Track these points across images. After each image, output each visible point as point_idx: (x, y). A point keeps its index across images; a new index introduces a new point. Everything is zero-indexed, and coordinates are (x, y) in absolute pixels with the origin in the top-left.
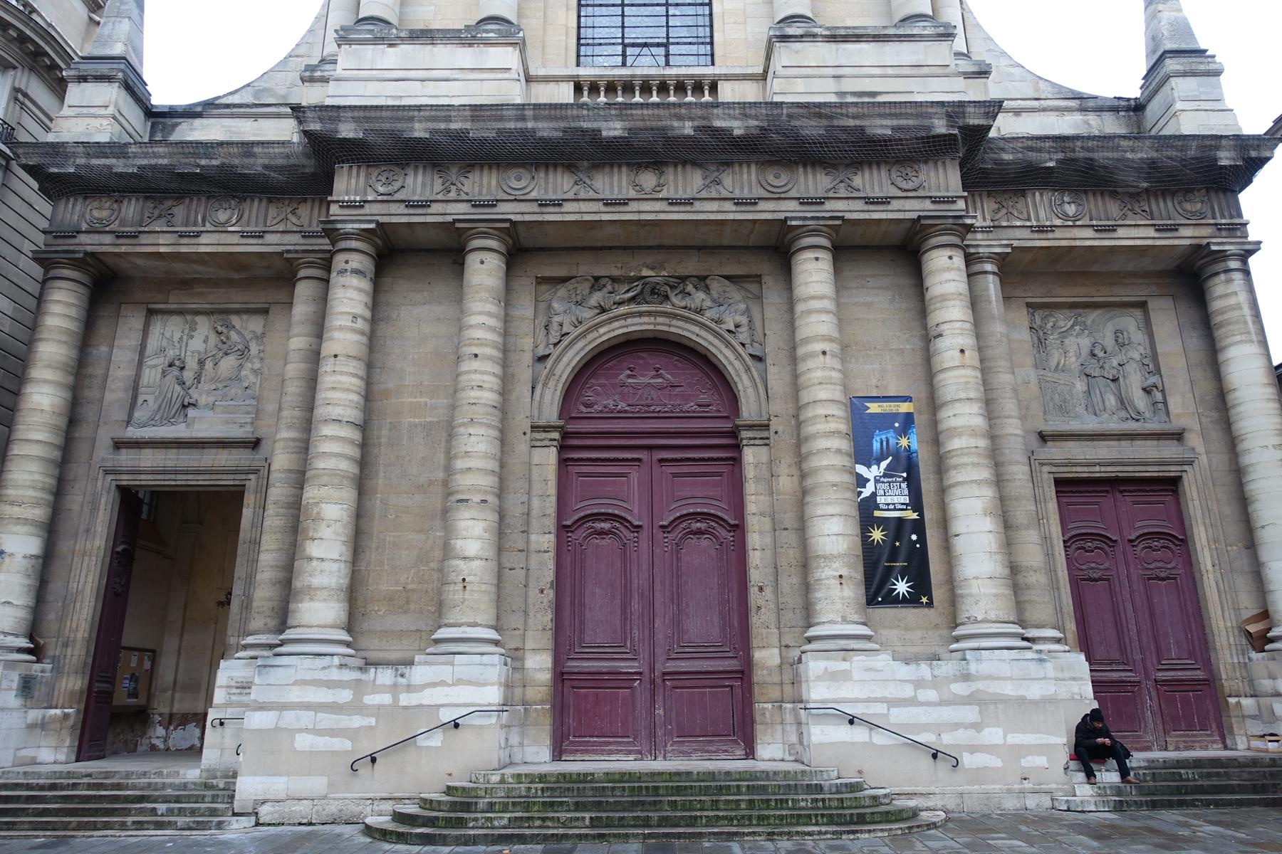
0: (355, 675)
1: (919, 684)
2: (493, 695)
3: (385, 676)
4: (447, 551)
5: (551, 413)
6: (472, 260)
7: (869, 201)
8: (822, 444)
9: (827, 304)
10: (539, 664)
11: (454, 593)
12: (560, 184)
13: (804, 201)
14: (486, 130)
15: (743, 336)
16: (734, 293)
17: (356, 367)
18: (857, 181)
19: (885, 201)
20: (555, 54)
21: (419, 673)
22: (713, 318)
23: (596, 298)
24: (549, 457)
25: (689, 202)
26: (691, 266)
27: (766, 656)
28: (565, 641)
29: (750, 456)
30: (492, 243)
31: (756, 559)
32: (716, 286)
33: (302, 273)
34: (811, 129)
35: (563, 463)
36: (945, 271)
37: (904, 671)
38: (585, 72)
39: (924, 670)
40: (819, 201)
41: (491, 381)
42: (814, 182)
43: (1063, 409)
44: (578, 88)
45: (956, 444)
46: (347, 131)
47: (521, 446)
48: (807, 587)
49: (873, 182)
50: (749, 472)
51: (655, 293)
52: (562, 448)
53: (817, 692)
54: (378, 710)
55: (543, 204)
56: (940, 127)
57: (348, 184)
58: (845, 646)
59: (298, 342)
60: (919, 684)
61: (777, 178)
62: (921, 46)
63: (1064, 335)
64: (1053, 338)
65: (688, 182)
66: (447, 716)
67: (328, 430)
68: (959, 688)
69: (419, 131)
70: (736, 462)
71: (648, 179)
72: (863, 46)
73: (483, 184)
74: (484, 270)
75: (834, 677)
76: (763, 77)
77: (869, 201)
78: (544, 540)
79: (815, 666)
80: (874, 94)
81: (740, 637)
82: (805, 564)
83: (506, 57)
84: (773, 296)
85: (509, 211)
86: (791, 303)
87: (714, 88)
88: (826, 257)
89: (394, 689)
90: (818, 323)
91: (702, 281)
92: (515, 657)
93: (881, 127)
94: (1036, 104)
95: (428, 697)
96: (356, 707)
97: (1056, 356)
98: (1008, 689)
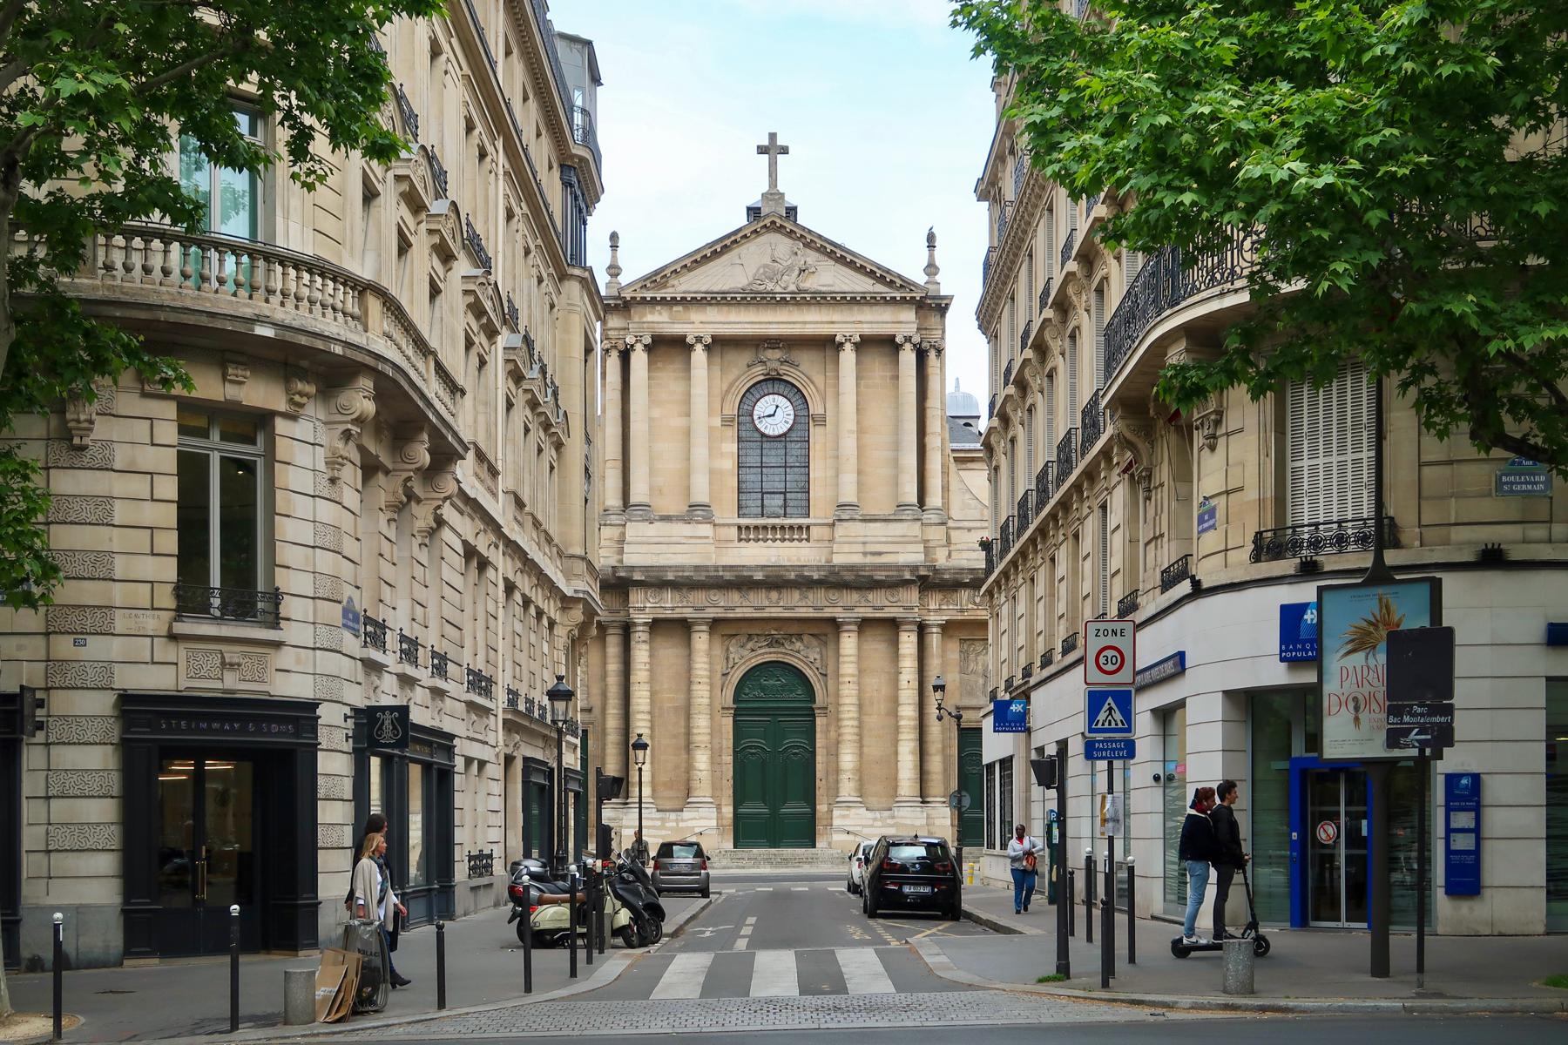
0: (659, 815)
1: (875, 819)
2: (714, 823)
3: (673, 816)
4: (690, 768)
5: (729, 702)
6: (695, 636)
7: (875, 608)
8: (845, 723)
9: (853, 659)
10: (728, 811)
11: (695, 784)
12: (735, 598)
13: (846, 608)
14: (702, 577)
15: (818, 664)
16: (815, 642)
17: (647, 687)
18: (870, 597)
19: (882, 608)
20: (727, 512)
21: (686, 814)
22: (804, 656)
23: (750, 645)
24: (728, 722)
25: (792, 608)
26: (794, 629)
27: (821, 808)
28: (737, 802)
29: (819, 721)
30: (704, 628)
31: (819, 767)
32: (805, 638)
33: (610, 631)
34: (848, 576)
35: (735, 721)
36: (908, 642)
37: (870, 814)
38: (744, 521)
39: (878, 814)
40: (851, 608)
41: (707, 694)
42: (852, 597)
43: (971, 693)
44: (739, 528)
45: (902, 723)
46: (637, 576)
47: (718, 716)
48: (837, 782)
49: (877, 597)
50: (818, 729)
51: (775, 642)
52: (735, 716)
53: (836, 822)
54: (671, 829)
55: (727, 609)
56: (907, 576)
57: (637, 598)
58: (848, 805)
59: (613, 666)
60: (875, 819)
61: (834, 595)
62: (905, 524)
63: (978, 654)
64: (972, 656)
65: (794, 597)
66: (697, 830)
67: (640, 716)
68: (890, 821)
69: (670, 576)
70: (814, 722)
71: (774, 595)
72: (878, 525)
73: (699, 597)
74: (701, 640)
75: (844, 817)
76: (833, 525)
77: (875, 608)
78: (728, 759)
79: (836, 813)
80: (880, 554)
81: (810, 798)
82: (838, 771)
83: (706, 530)
84: (831, 646)
85: (711, 613)
86: (838, 654)
87: (808, 528)
88: (854, 635)
89: (677, 821)
90: (848, 668)
91: (799, 637)
92: (719, 807)
93: (880, 576)
94: (979, 524)
95: (690, 824)
96: (663, 827)
97: (972, 666)
98: (908, 822)
